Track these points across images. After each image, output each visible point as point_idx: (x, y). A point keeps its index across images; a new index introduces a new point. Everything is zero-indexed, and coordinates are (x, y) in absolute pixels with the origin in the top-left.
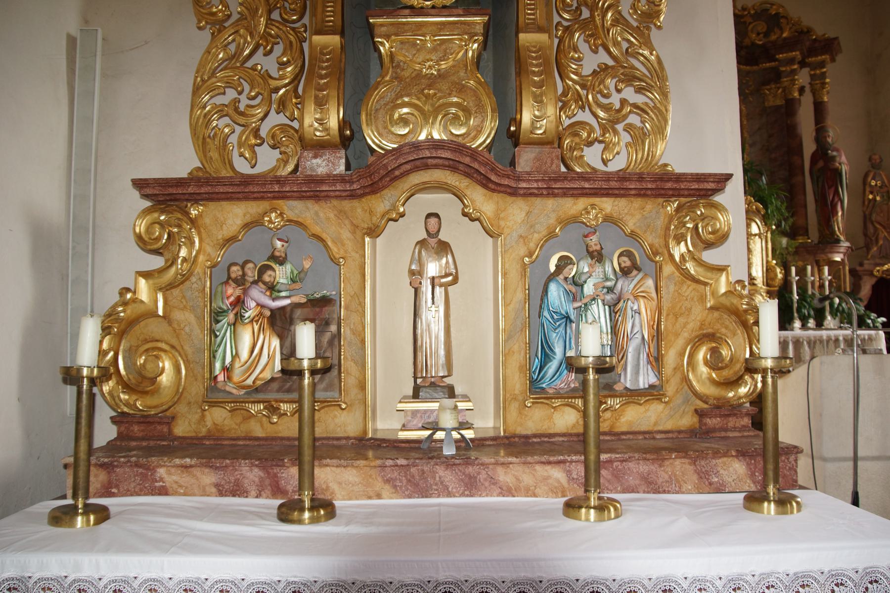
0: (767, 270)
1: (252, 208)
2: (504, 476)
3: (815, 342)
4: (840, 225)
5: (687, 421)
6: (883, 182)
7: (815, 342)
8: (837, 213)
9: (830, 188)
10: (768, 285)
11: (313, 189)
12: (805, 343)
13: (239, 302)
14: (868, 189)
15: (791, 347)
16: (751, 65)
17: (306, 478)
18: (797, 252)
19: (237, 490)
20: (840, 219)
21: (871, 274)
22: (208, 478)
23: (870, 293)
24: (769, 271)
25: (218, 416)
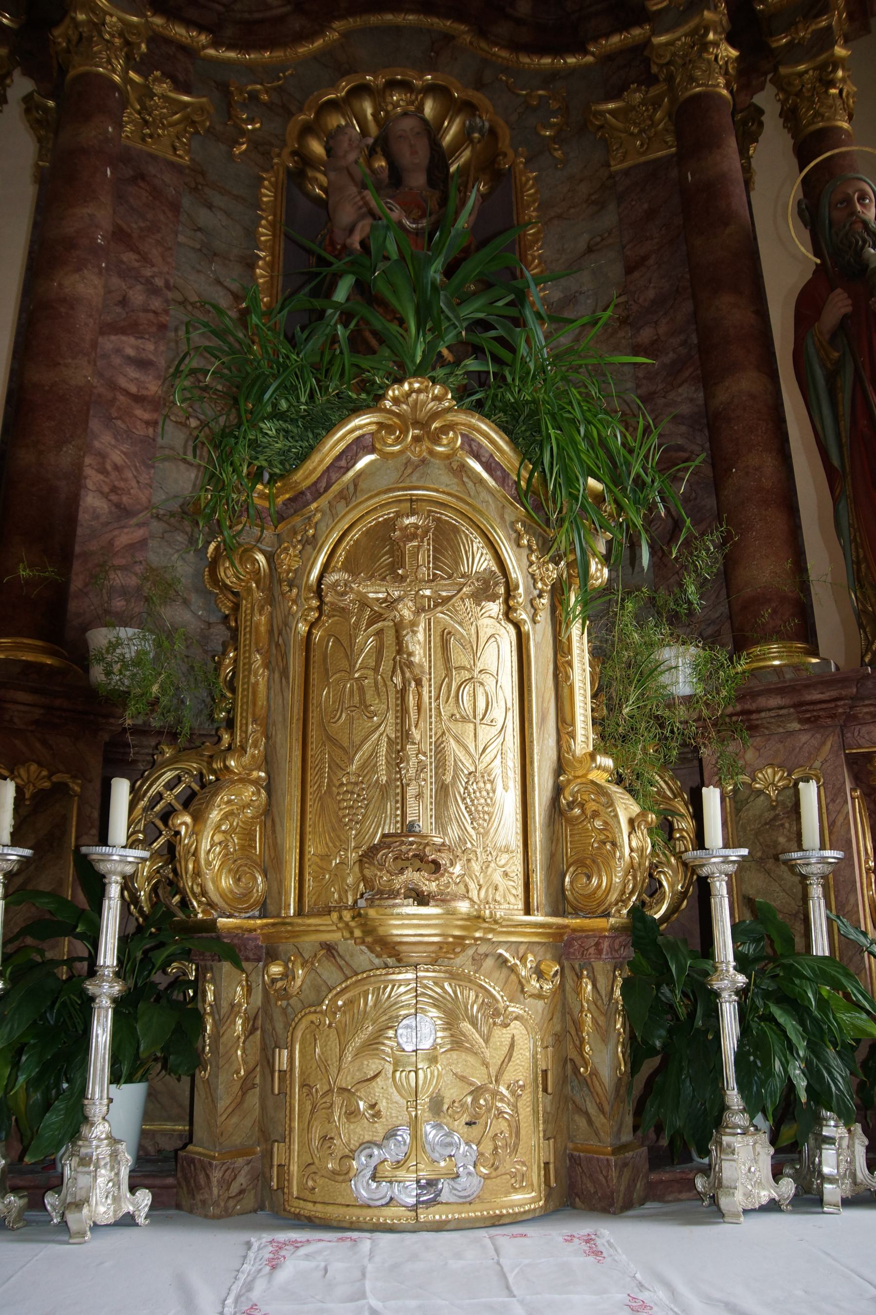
0: (557, 809)
10: (560, 903)
16: (558, 51)
24: (565, 825)
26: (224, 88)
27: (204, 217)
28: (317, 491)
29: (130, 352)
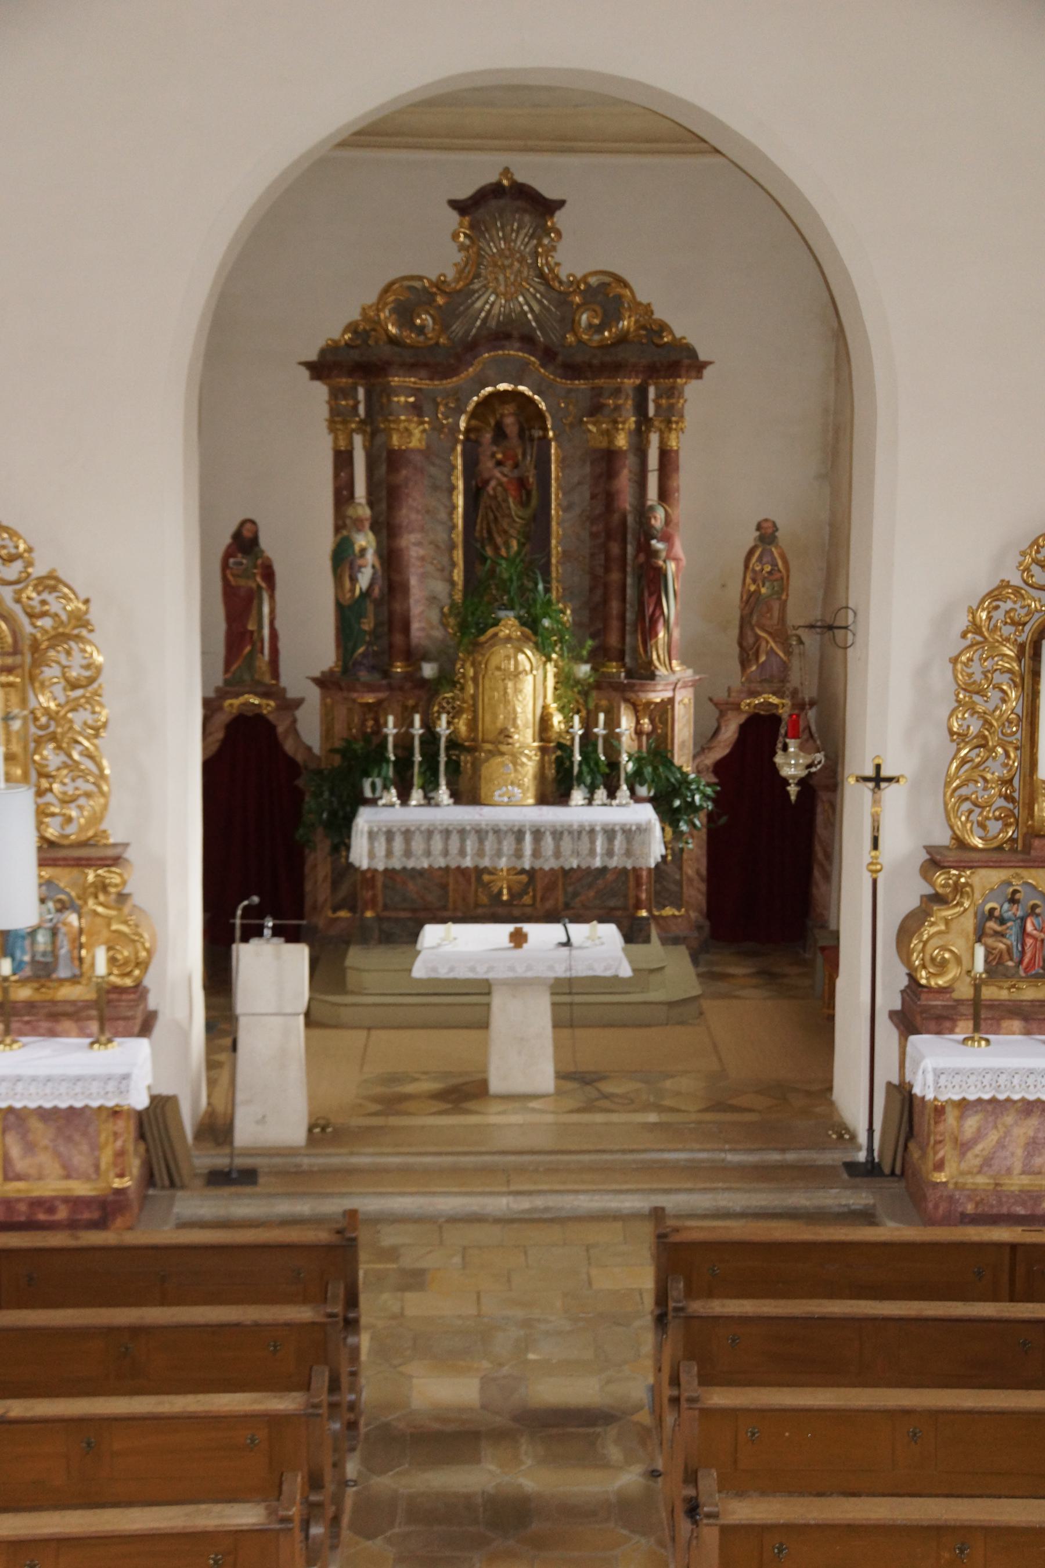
3: (562, 833)
4: (661, 652)
6: (774, 564)
7: (562, 833)
8: (656, 635)
9: (651, 595)
10: (542, 740)
12: (548, 833)
14: (749, 575)
18: (598, 686)
20: (661, 642)
21: (737, 707)
23: (736, 736)
24: (544, 723)
26: (434, 400)
27: (433, 470)
28: (486, 642)
29: (413, 540)
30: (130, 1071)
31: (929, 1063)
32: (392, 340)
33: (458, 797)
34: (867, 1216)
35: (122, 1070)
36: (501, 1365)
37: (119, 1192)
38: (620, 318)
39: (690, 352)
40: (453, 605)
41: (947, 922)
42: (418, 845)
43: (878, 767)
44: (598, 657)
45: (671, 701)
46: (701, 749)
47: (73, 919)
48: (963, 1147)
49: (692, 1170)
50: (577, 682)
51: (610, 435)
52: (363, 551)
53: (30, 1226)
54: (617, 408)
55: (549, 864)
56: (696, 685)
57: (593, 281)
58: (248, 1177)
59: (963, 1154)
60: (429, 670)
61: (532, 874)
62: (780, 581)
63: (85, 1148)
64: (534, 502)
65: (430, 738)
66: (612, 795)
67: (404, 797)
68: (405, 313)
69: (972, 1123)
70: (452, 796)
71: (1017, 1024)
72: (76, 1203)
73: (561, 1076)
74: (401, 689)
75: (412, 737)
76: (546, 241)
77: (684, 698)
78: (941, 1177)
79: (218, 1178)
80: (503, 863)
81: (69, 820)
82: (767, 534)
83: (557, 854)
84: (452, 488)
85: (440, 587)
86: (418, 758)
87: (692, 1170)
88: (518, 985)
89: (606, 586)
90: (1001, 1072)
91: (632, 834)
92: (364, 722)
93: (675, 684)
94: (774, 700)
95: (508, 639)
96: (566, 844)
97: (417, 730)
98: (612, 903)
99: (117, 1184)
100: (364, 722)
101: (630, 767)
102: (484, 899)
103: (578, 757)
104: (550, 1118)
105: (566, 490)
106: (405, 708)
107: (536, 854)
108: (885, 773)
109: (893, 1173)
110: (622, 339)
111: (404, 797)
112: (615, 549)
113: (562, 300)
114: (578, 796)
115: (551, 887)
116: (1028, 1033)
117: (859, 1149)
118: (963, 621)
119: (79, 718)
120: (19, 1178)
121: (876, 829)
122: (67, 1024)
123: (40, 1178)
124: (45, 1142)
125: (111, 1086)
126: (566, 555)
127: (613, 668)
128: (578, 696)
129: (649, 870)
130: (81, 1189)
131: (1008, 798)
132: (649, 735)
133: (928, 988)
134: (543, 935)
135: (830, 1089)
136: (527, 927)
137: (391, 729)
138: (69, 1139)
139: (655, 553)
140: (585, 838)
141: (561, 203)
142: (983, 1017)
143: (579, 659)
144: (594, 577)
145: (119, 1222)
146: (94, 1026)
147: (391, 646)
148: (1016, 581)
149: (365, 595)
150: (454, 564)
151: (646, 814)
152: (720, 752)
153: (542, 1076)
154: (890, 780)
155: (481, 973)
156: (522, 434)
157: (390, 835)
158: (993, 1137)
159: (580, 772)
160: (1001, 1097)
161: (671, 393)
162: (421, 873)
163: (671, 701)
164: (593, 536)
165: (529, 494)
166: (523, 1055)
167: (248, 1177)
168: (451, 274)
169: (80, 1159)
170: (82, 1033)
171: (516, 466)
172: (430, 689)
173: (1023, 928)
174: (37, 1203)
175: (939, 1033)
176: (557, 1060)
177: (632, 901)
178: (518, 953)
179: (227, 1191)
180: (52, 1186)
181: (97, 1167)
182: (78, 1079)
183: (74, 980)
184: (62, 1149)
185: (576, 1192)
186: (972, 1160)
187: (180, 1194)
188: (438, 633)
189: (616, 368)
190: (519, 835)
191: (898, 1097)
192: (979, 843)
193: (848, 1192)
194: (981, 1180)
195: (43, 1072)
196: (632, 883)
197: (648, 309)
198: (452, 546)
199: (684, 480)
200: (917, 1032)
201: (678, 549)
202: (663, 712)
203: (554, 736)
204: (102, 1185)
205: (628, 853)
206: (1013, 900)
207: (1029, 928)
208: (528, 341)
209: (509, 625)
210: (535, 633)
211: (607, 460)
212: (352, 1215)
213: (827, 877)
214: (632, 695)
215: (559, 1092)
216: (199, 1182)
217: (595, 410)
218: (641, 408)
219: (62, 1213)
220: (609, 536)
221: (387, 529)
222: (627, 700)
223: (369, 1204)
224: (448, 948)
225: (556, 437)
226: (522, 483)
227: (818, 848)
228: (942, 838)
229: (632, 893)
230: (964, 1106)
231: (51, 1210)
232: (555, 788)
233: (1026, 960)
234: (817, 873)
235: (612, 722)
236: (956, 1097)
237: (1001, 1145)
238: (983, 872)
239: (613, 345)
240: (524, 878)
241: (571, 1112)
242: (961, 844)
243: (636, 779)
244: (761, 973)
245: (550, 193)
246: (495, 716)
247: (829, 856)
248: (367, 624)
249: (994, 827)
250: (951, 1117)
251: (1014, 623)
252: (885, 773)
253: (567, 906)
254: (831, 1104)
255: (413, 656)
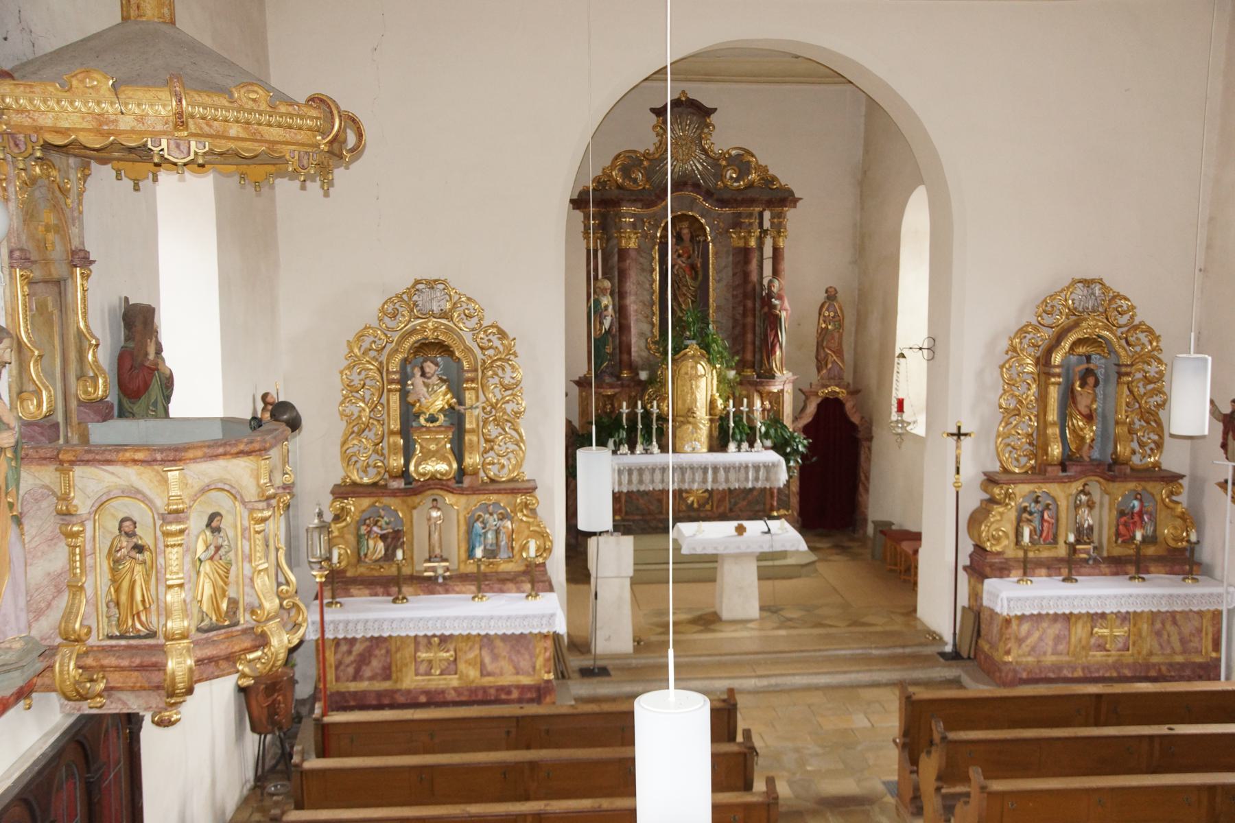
1: (373, 500)
2: (457, 589)
5: (522, 568)
6: (836, 312)
11: (395, 493)
13: (369, 532)
15: (710, 472)
17: (400, 592)
18: (741, 383)
19: (376, 595)
21: (817, 394)
22: (367, 592)
24: (712, 404)
25: (362, 570)
27: (642, 260)
30: (547, 612)
31: (1004, 595)
32: (619, 187)
33: (663, 449)
34: (956, 683)
35: (551, 612)
36: (794, 774)
37: (548, 681)
38: (749, 173)
39: (791, 193)
40: (653, 336)
41: (1001, 514)
42: (647, 477)
43: (959, 428)
44: (741, 366)
45: (782, 391)
46: (795, 419)
47: (509, 524)
48: (1020, 641)
49: (854, 659)
50: (729, 381)
51: (746, 240)
52: (606, 307)
53: (497, 701)
54: (751, 224)
55: (722, 486)
56: (794, 382)
57: (734, 152)
58: (603, 672)
59: (1020, 646)
60: (643, 375)
61: (711, 493)
62: (839, 321)
63: (527, 657)
64: (700, 278)
65: (647, 414)
66: (751, 445)
67: (632, 449)
68: (626, 171)
69: (1025, 627)
70: (659, 447)
71: (1044, 571)
72: (523, 688)
73: (762, 609)
74: (628, 386)
75: (636, 414)
76: (706, 130)
77: (788, 388)
78: (1009, 658)
79: (586, 673)
80: (695, 486)
81: (503, 466)
82: (831, 296)
83: (727, 480)
84: (653, 270)
85: (646, 327)
86: (640, 426)
87: (854, 659)
88: (739, 557)
89: (744, 326)
90: (1043, 598)
91: (770, 468)
92: (605, 406)
93: (783, 382)
94: (837, 389)
95: (693, 357)
96: (732, 476)
97: (640, 410)
98: (757, 508)
99: (546, 677)
100: (605, 406)
101: (763, 429)
102: (684, 508)
103: (732, 424)
104: (756, 633)
105: (718, 271)
106: (630, 397)
107: (715, 480)
108: (962, 431)
109: (969, 658)
110: (751, 186)
111: (632, 449)
112: (749, 304)
113: (714, 161)
114: (732, 446)
115: (721, 501)
116: (1049, 576)
117: (946, 644)
118: (1004, 344)
119: (509, 408)
120: (489, 674)
121: (958, 462)
122: (510, 585)
123: (502, 674)
124: (504, 654)
125: (544, 622)
126: (718, 308)
127: (748, 372)
128: (730, 390)
129: (779, 489)
130: (526, 680)
131: (1031, 444)
132: (769, 411)
133: (991, 552)
134: (754, 527)
135: (915, 610)
136: (746, 523)
137: (625, 410)
138: (518, 652)
139: (775, 307)
140: (743, 471)
141: (715, 109)
142: (1027, 567)
143: (729, 368)
144: (735, 321)
145: (548, 699)
146: (528, 586)
147: (621, 361)
148: (1034, 322)
149: (608, 332)
150: (653, 314)
151: (773, 457)
152: (807, 419)
153: (752, 609)
154: (965, 435)
155: (710, 551)
156: (692, 239)
157: (630, 472)
158: (1036, 635)
159: (734, 433)
160: (1044, 612)
161: (780, 215)
162: (646, 493)
163: (782, 391)
164: (734, 296)
165: (696, 273)
166: (740, 595)
167: (603, 672)
168: (652, 149)
169: (524, 664)
170: (519, 590)
171: (689, 257)
172: (643, 385)
173: (1042, 517)
174: (501, 689)
175: (1001, 577)
176: (761, 599)
177: (768, 507)
178: (740, 538)
179: (595, 680)
180: (508, 679)
181: (534, 668)
182: (526, 617)
183: (510, 559)
184: (514, 658)
185: (794, 675)
186: (1025, 648)
187: (569, 682)
188: (645, 354)
189: (751, 202)
190: (705, 470)
191: (971, 616)
192: (1017, 470)
193: (946, 669)
194: (1030, 659)
195: (522, 613)
196: (768, 497)
197: (765, 169)
198: (653, 304)
199: (787, 265)
200: (987, 577)
201: (786, 305)
202: (777, 398)
203: (718, 412)
204: (536, 677)
205: (767, 479)
206: (1037, 501)
207: (1046, 517)
208: (696, 186)
209: (693, 348)
210: (708, 352)
211: (744, 255)
212: (731, 691)
213: (867, 490)
214: (760, 388)
215: (761, 618)
216: (577, 675)
217: (737, 225)
218: (761, 225)
219: (515, 695)
220: (745, 296)
221: (620, 295)
222: (758, 391)
223: (735, 684)
224: (699, 536)
225: (712, 241)
226: (693, 267)
227: (862, 475)
228: (996, 467)
229: (768, 501)
230: (1022, 618)
231: (509, 693)
232: (719, 442)
233: (1044, 534)
234: (861, 488)
235: (751, 405)
236: (1019, 613)
237: (1041, 639)
238: (1021, 486)
239: (746, 188)
240: (706, 495)
241: (774, 629)
242: (1006, 471)
243: (766, 435)
244: (836, 546)
245: (708, 104)
246: (684, 401)
247: (867, 478)
248: (609, 349)
249: (1023, 460)
250: (1014, 624)
251: (1034, 346)
252: (962, 431)
253: (731, 510)
254: (916, 619)
255: (634, 369)
